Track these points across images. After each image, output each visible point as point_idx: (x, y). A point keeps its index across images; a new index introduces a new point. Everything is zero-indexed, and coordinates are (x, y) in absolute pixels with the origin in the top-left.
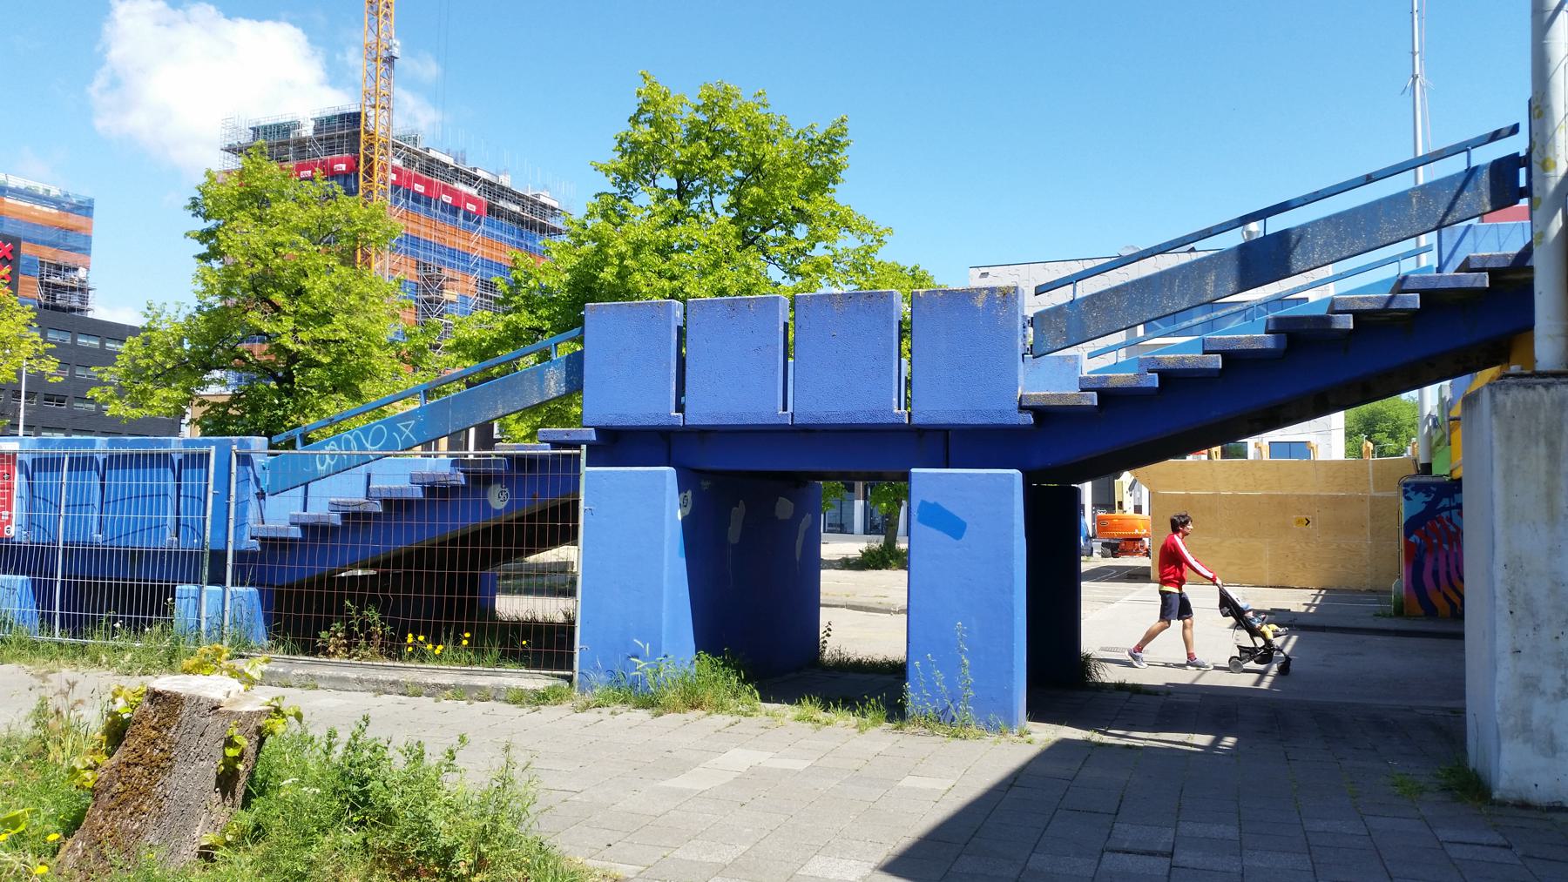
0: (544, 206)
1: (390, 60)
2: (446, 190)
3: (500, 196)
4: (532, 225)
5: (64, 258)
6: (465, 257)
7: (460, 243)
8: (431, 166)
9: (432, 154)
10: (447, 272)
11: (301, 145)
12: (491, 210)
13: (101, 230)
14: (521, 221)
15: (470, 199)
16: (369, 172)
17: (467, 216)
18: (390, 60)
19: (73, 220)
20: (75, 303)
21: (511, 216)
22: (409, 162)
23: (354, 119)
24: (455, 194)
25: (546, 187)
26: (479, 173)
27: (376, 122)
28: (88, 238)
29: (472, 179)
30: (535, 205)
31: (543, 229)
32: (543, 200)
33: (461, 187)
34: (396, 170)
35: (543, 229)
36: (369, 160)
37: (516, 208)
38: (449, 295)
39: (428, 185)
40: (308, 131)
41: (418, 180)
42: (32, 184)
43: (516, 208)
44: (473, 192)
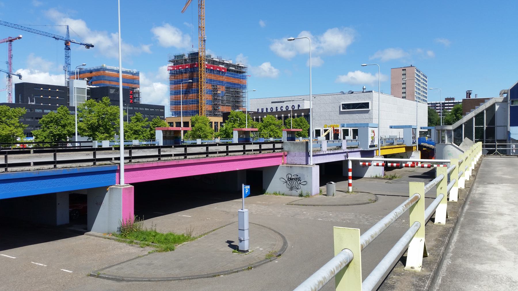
0: (240, 67)
1: (204, 41)
2: (217, 67)
3: (230, 66)
4: (237, 72)
5: (134, 86)
6: (222, 82)
7: (221, 79)
8: (214, 62)
9: (214, 59)
10: (218, 87)
11: (185, 60)
12: (228, 70)
13: (142, 78)
14: (235, 71)
15: (223, 68)
16: (201, 67)
17: (222, 72)
18: (204, 41)
19: (135, 77)
20: (137, 96)
21: (232, 71)
22: (209, 62)
23: (197, 54)
24: (219, 68)
25: (241, 61)
26: (225, 62)
27: (200, 54)
28: (139, 81)
29: (223, 64)
30: (238, 67)
31: (240, 72)
32: (240, 65)
33: (221, 66)
34: (207, 65)
35: (240, 72)
36: (201, 64)
37: (234, 69)
38: (219, 92)
39: (213, 67)
40: (186, 57)
41: (211, 66)
42: (126, 69)
43: (234, 69)
44: (223, 66)
